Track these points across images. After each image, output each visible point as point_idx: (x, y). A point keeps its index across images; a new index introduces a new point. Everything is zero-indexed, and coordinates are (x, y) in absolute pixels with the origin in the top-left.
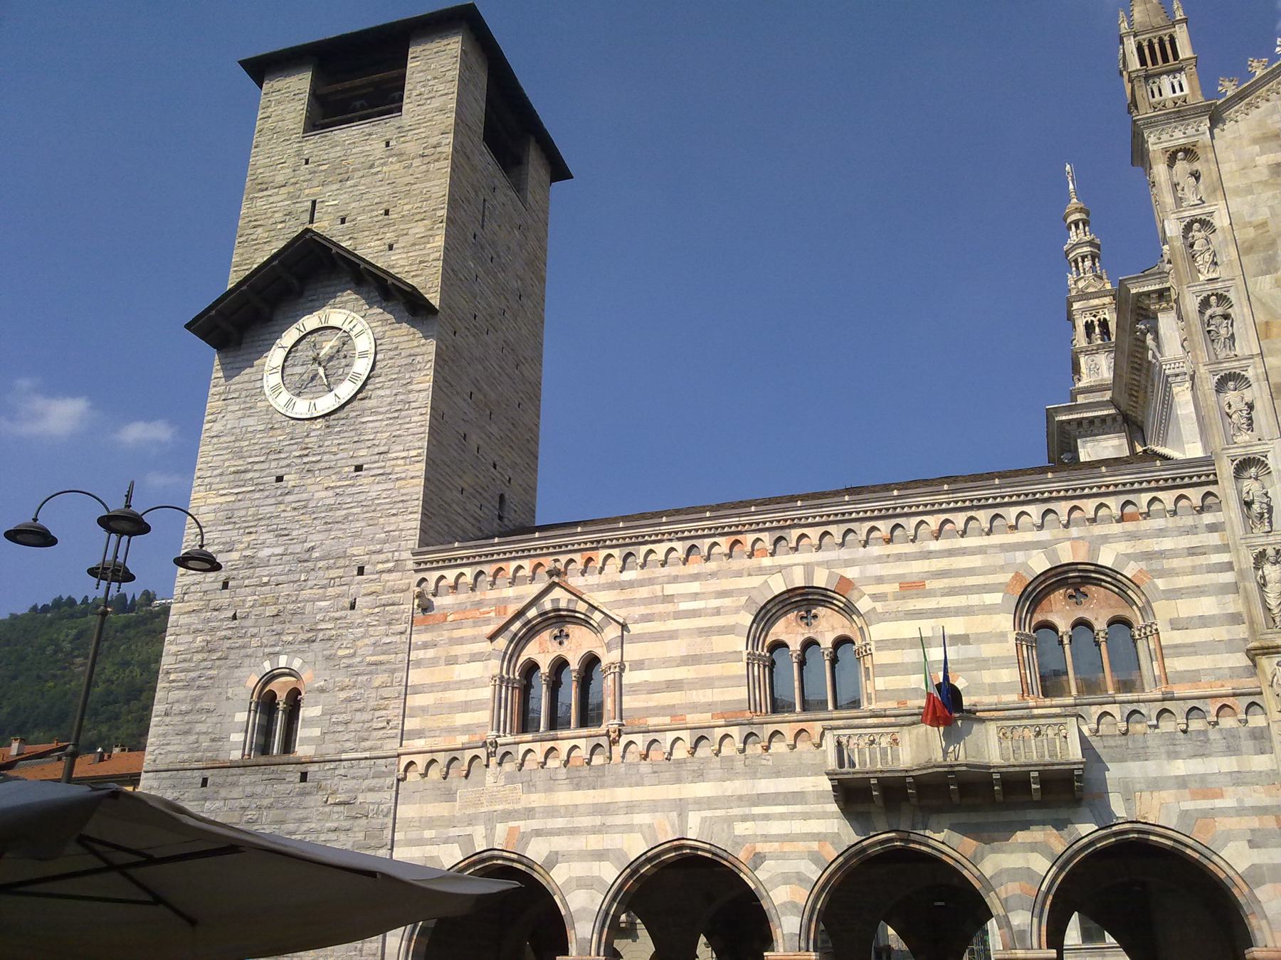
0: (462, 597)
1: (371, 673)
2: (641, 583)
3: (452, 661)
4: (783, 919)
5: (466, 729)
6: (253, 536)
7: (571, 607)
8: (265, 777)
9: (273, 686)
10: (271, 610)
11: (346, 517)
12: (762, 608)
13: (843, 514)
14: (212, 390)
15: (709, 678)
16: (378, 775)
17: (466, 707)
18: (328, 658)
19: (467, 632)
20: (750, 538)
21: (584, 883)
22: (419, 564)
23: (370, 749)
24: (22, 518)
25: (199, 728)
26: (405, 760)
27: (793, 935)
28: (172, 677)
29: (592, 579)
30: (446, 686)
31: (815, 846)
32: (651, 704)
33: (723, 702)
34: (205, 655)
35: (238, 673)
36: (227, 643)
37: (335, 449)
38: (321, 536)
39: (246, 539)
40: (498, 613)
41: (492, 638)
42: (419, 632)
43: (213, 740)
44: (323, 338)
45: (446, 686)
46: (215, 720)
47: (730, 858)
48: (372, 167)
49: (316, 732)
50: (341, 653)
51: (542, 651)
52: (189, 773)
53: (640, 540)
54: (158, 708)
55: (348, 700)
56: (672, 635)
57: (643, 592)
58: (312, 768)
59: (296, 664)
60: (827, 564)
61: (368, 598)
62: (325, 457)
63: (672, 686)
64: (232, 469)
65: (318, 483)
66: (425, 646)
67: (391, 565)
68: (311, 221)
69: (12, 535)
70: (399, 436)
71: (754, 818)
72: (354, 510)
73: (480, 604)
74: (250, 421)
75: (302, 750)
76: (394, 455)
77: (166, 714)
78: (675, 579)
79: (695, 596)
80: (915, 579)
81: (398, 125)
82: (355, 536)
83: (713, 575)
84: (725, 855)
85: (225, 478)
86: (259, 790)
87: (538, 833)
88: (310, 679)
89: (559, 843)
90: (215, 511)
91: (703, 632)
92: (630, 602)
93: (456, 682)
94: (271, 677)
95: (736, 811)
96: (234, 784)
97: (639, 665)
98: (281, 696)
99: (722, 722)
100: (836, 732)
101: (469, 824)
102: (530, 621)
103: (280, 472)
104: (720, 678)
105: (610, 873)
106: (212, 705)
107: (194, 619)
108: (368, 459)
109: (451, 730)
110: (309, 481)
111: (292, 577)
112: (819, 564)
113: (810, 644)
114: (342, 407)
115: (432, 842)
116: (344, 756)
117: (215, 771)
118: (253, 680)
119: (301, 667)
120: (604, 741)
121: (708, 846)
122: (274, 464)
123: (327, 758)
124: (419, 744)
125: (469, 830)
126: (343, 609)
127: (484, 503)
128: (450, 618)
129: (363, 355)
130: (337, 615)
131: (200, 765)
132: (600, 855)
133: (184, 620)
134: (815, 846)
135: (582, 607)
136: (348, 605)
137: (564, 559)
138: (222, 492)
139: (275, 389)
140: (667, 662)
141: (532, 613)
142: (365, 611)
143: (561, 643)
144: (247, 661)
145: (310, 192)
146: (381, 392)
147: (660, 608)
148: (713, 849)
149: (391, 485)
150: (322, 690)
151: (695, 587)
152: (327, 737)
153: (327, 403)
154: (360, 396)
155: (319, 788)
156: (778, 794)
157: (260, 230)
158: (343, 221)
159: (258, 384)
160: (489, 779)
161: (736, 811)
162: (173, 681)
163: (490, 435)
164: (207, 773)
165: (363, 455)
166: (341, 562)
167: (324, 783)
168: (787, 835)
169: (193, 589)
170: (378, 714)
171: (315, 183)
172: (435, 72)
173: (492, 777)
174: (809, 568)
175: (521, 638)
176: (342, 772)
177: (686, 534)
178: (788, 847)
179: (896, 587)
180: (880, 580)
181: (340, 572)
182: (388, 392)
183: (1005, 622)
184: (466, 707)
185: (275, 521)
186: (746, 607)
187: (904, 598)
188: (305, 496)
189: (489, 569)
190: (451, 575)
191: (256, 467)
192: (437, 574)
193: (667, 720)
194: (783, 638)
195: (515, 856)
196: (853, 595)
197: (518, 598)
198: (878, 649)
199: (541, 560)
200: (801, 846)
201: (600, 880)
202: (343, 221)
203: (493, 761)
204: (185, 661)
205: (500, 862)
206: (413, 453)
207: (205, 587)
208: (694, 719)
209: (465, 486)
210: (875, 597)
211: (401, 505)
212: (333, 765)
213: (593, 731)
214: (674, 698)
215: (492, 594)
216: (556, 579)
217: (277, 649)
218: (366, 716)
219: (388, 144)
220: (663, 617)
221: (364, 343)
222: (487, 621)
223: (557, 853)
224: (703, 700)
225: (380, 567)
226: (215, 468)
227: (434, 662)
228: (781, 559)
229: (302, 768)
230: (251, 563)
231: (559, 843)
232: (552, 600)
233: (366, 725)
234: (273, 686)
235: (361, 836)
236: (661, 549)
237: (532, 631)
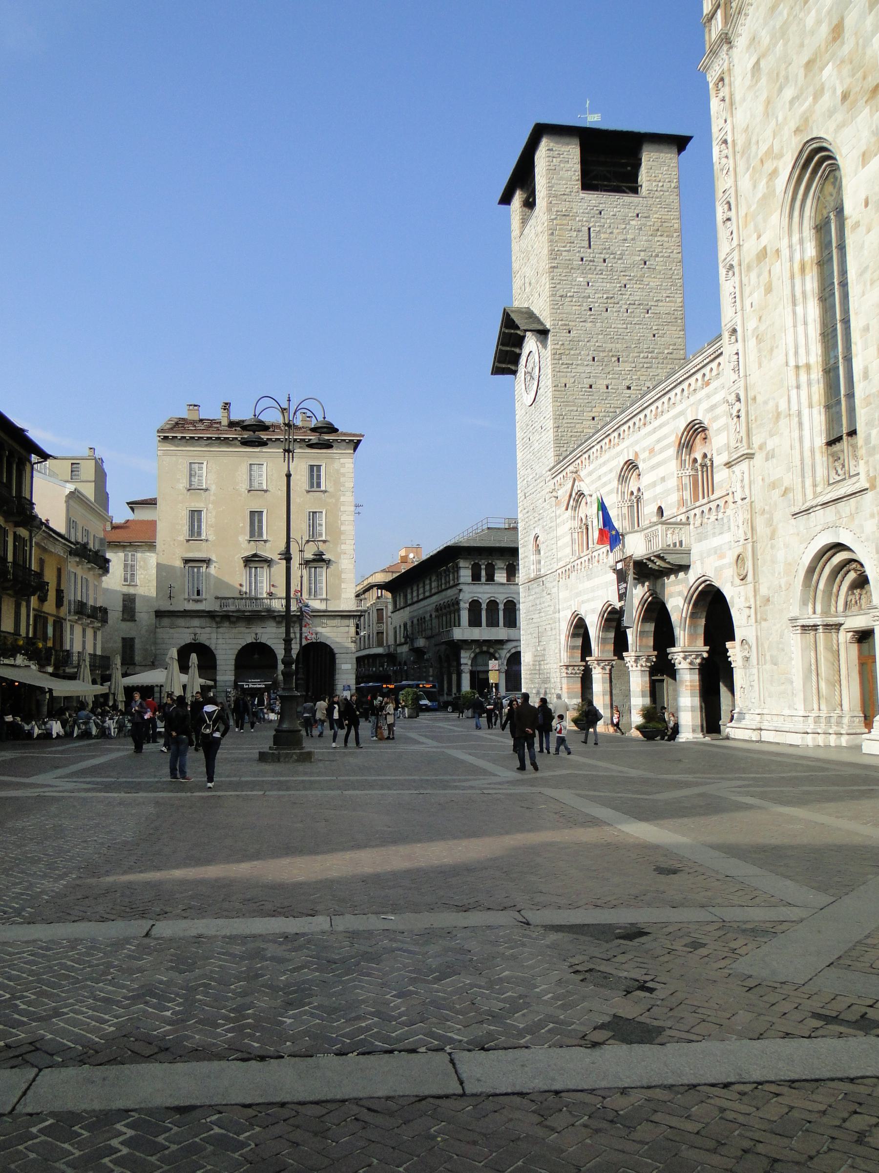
41: (567, 509)
87: (583, 602)
151: (604, 469)
173: (573, 575)
183: (673, 466)
209: (593, 415)
210: (644, 460)
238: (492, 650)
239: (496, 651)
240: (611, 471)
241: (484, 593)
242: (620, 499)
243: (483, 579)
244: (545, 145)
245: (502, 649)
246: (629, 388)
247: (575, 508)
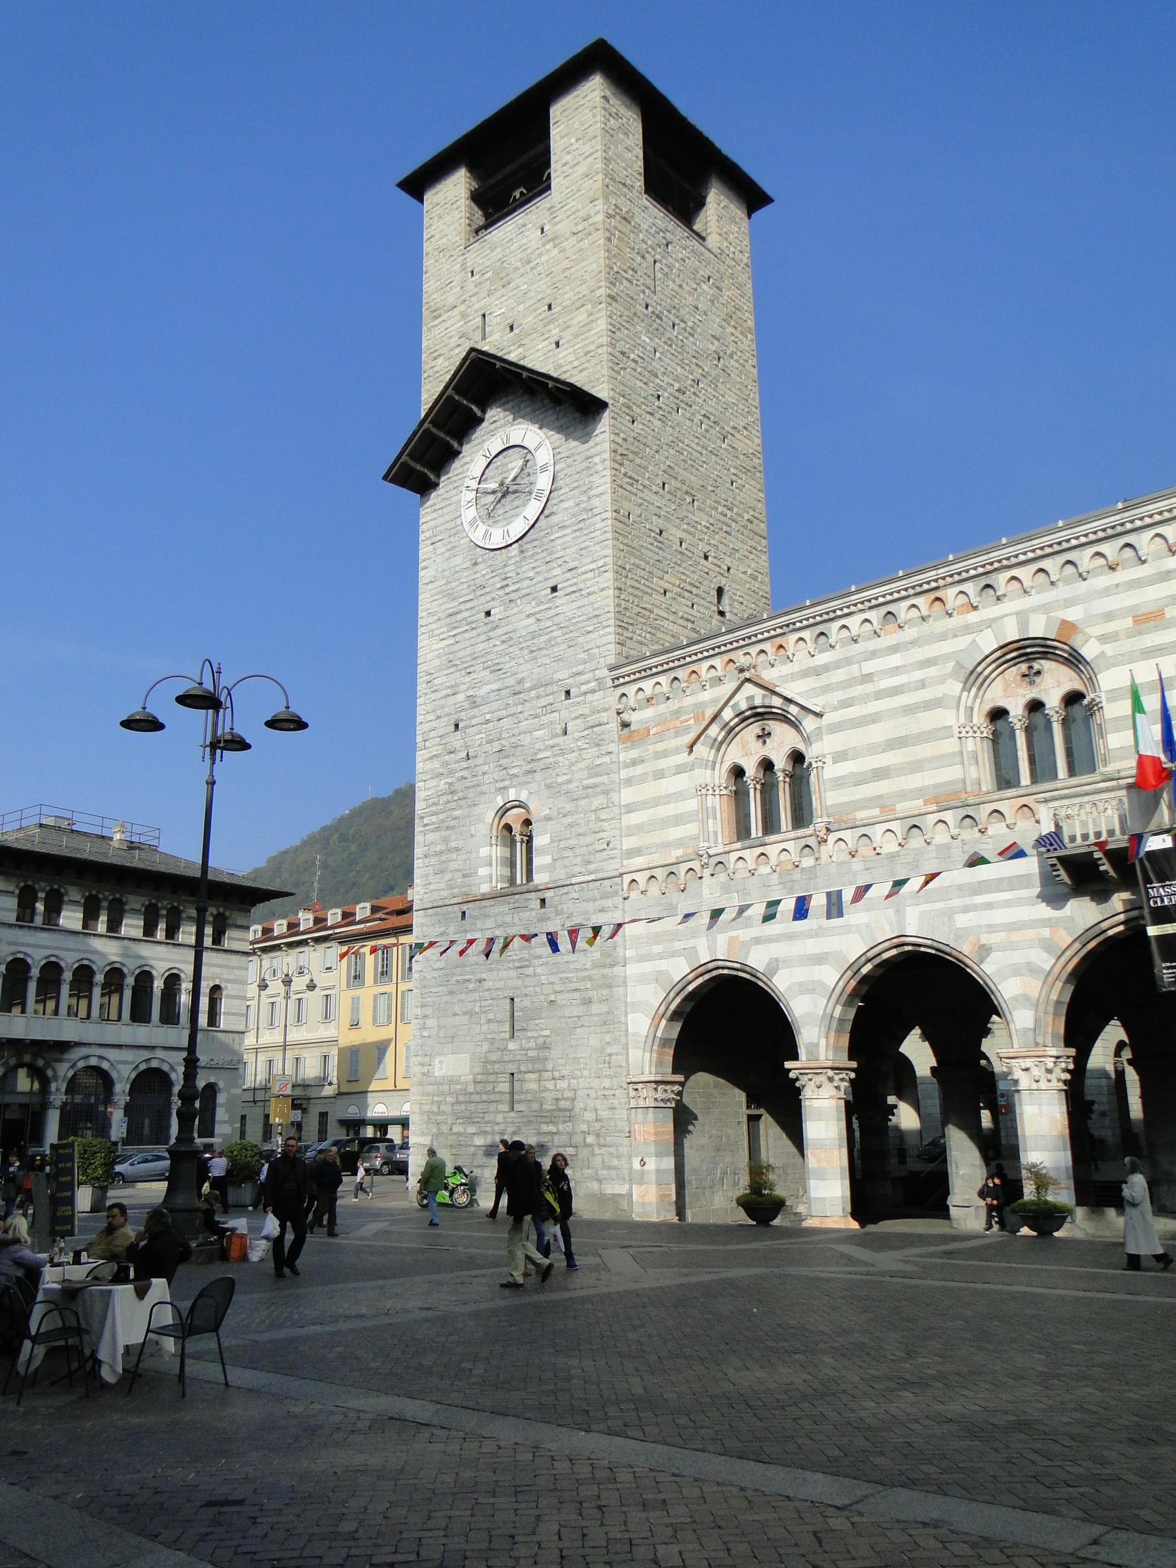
0: (663, 708)
1: (587, 797)
2: (837, 665)
3: (659, 775)
4: (1014, 1013)
5: (679, 843)
6: (473, 676)
7: (767, 703)
8: (511, 906)
9: (510, 818)
10: (496, 746)
11: (550, 640)
12: (972, 672)
13: (1059, 543)
14: (422, 537)
15: (917, 761)
16: (605, 896)
17: (679, 820)
18: (548, 786)
19: (673, 743)
20: (950, 594)
21: (807, 988)
22: (618, 679)
23: (597, 871)
24: (132, 709)
25: (454, 866)
26: (627, 879)
27: (1026, 1030)
28: (426, 821)
29: (787, 669)
30: (657, 802)
31: (1046, 932)
32: (858, 797)
33: (935, 786)
34: (449, 797)
35: (477, 810)
36: (467, 783)
37: (531, 574)
38: (529, 666)
39: (467, 679)
40: (697, 719)
42: (626, 750)
43: (464, 876)
44: (506, 460)
45: (657, 802)
46: (464, 857)
47: (954, 953)
49: (548, 859)
50: (560, 780)
51: (746, 752)
52: (450, 909)
53: (832, 615)
54: (418, 851)
55: (571, 826)
56: (874, 719)
57: (840, 675)
58: (548, 895)
59: (523, 797)
60: (1044, 608)
61: (578, 721)
62: (526, 583)
63: (880, 774)
64: (447, 612)
65: (520, 612)
66: (634, 763)
67: (593, 684)
68: (484, 338)
69: (128, 724)
70: (587, 547)
71: (975, 908)
72: (554, 634)
73: (677, 713)
74: (458, 560)
75: (539, 878)
76: (583, 570)
77: (426, 856)
78: (873, 655)
79: (897, 671)
80: (1152, 608)
81: (548, 205)
82: (558, 660)
83: (913, 643)
84: (948, 949)
85: (443, 622)
86: (508, 919)
87: (757, 941)
88: (537, 811)
89: (778, 950)
90: (439, 656)
91: (910, 710)
92: (827, 689)
93: (665, 797)
94: (504, 811)
95: (956, 903)
96: (485, 916)
97: (841, 756)
98: (517, 828)
99: (933, 808)
100: (1051, 804)
101: (693, 937)
102: (727, 724)
104: (929, 760)
105: (832, 978)
106: (460, 844)
107: (436, 764)
108: (559, 579)
109: (666, 845)
110: (513, 612)
111: (511, 710)
112: (1035, 609)
113: (1035, 706)
115: (660, 956)
116: (573, 881)
117: (471, 905)
118: (490, 815)
119: (528, 798)
120: (812, 842)
121: (929, 942)
122: (482, 600)
123: (560, 883)
124: (639, 862)
125: (691, 943)
126: (556, 736)
127: (696, 600)
128: (652, 732)
129: (544, 469)
130: (551, 742)
131: (459, 900)
132: (819, 959)
133: (429, 766)
134: (1046, 932)
135: (777, 701)
136: (559, 731)
137: (753, 650)
138: (442, 636)
139: (473, 522)
140: (873, 749)
141: (728, 714)
142: (577, 735)
143: (765, 742)
144: (483, 798)
145: (478, 305)
146: (565, 505)
147: (858, 690)
148: (935, 944)
149: (585, 601)
150: (548, 819)
151: (895, 660)
152: (558, 863)
153: (518, 528)
154: (546, 512)
155: (557, 913)
156: (1001, 880)
158: (512, 328)
159: (458, 522)
160: (706, 891)
161: (956, 903)
162: (426, 825)
163: (694, 525)
164: (464, 907)
165: (557, 575)
166: (550, 689)
167: (560, 907)
168: (1014, 923)
169: (431, 735)
170: (599, 836)
171: (481, 295)
172: (590, 134)
174: (1022, 617)
175: (721, 743)
176: (575, 895)
177: (881, 600)
178: (1015, 937)
179: (1128, 622)
180: (1109, 616)
181: (550, 699)
182: (571, 503)
184: (679, 820)
185: (490, 657)
186: (954, 674)
187: (1140, 634)
188: (510, 628)
189: (682, 674)
190: (648, 685)
191: (468, 605)
192: (635, 687)
193: (876, 812)
194: (1002, 703)
195: (738, 966)
196: (1076, 642)
197: (714, 701)
198: (1110, 700)
199: (732, 655)
200: (1031, 933)
201: (820, 983)
202: (512, 328)
203: (707, 873)
204: (434, 804)
205: (726, 972)
206: (600, 563)
207: (441, 731)
208: (903, 808)
210: (1103, 639)
211: (595, 620)
212: (565, 890)
213: (801, 832)
214: (882, 787)
215: (688, 701)
216: (747, 675)
217: (507, 783)
218: (589, 839)
220: (865, 699)
221: (543, 456)
222: (687, 729)
223: (777, 960)
224: (913, 786)
225: (584, 688)
227: (643, 779)
228: (990, 611)
229: (541, 895)
230: (473, 702)
231: (778, 950)
232: (747, 698)
233: (591, 848)
234: (510, 818)
235: (597, 955)
236: (854, 622)
237: (730, 732)
238: (40, 1063)
239: (48, 1065)
240: (927, 663)
241: (38, 946)
242: (962, 721)
243: (39, 920)
244: (594, 89)
245: (61, 1061)
246: (706, 557)
247: (718, 745)
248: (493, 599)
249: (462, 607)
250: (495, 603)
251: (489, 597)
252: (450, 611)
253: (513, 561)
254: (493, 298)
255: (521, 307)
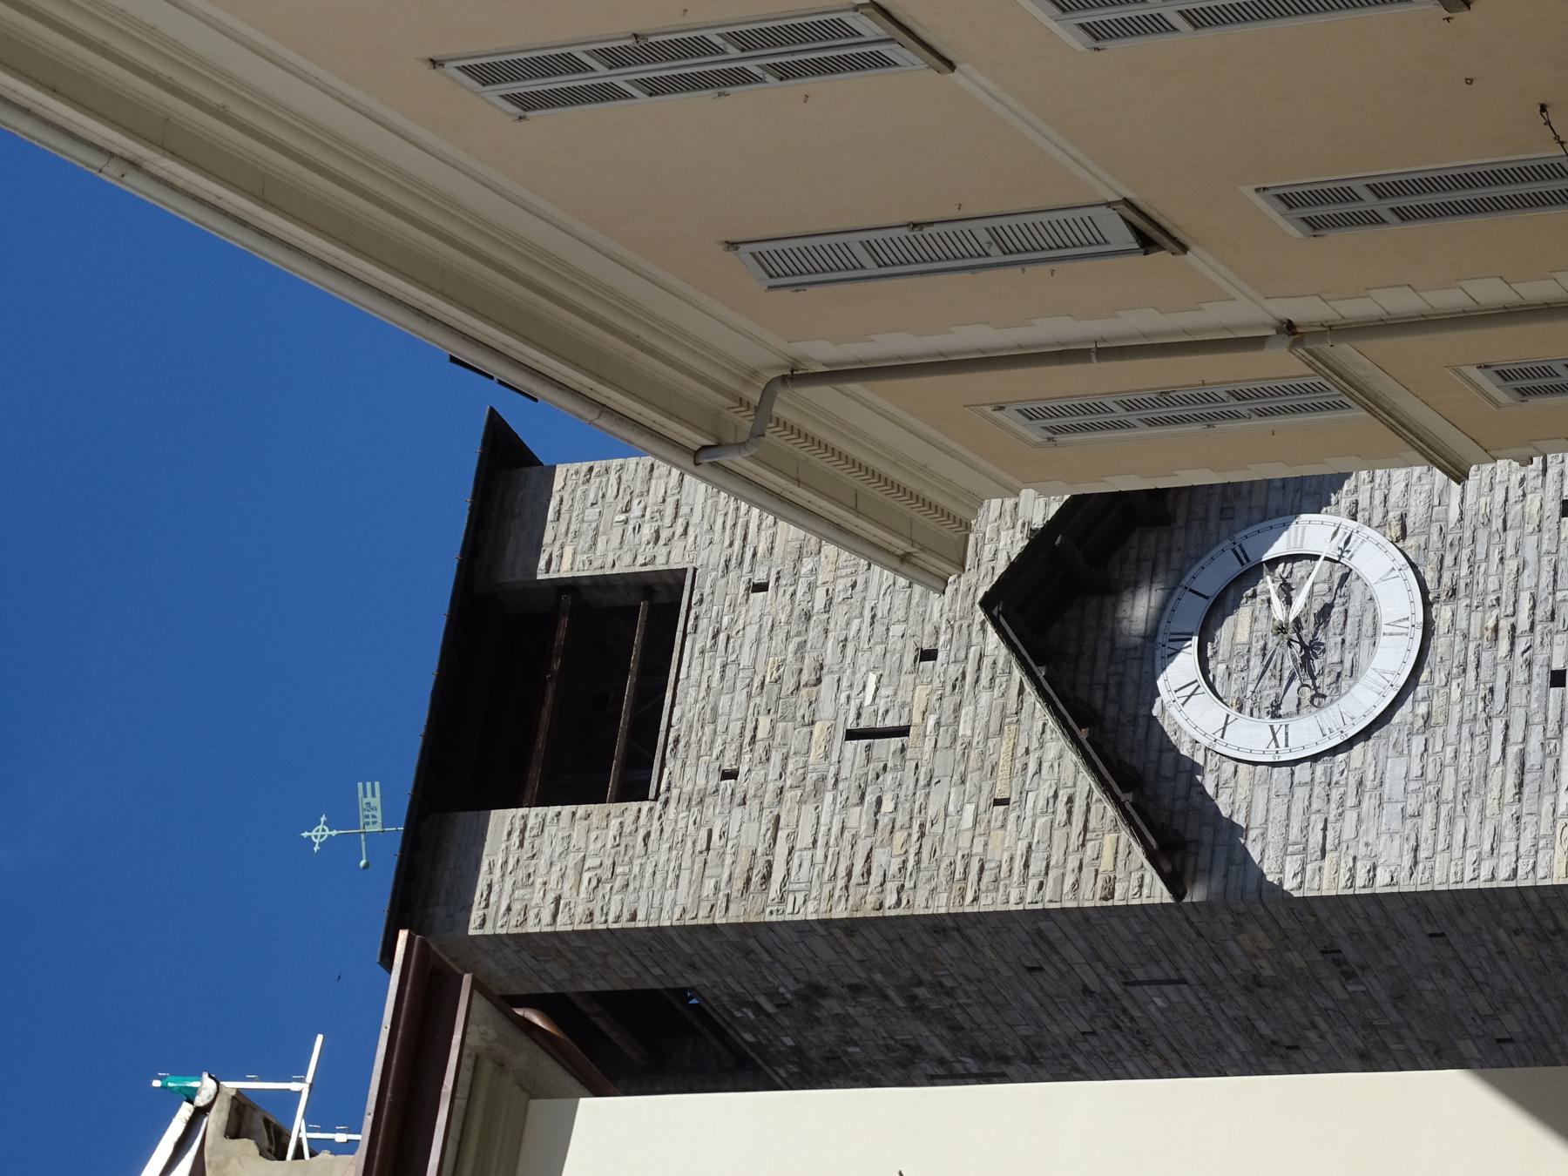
37: (1512, 565)
48: (808, 616)
62: (1527, 580)
74: (1395, 769)
103: (1541, 677)
114: (1413, 566)
122: (1518, 696)
157: (880, 857)
191: (1516, 734)
219: (761, 587)
226: (1497, 835)
248: (1529, 664)
249: (1513, 750)
250: (1540, 658)
251: (1520, 676)
252: (1511, 780)
253: (1462, 613)
254: (826, 710)
255: (896, 630)
